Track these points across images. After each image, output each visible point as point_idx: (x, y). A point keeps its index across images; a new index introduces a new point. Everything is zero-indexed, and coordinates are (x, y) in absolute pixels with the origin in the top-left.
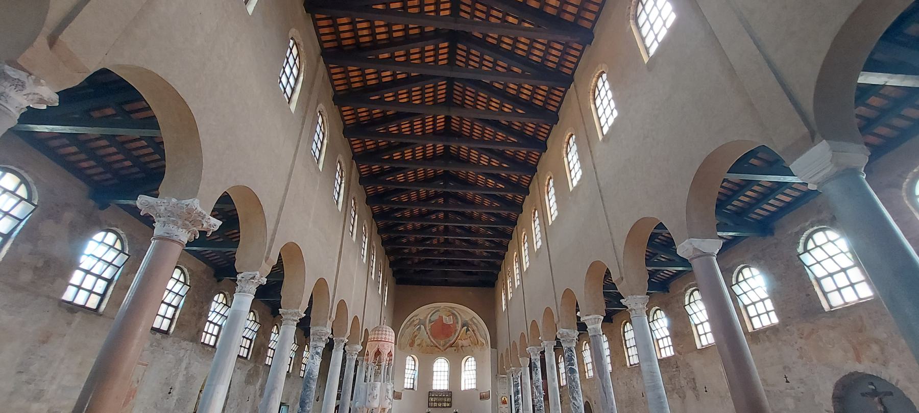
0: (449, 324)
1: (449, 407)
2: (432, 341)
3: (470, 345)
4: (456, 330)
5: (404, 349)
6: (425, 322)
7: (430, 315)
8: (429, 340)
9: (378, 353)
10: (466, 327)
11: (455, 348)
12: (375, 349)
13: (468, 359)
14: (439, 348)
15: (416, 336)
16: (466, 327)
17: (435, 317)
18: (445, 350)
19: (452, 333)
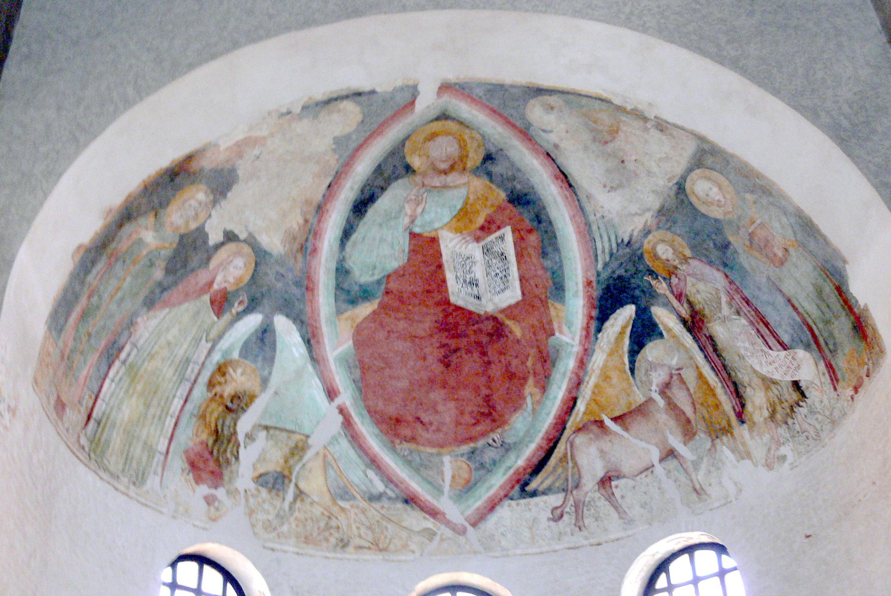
2: (374, 462)
5: (139, 479)
6: (307, 285)
8: (345, 444)
10: (628, 312)
11: (555, 500)
13: (662, 567)
14: (434, 513)
16: (628, 312)
18: (478, 520)
19: (525, 379)
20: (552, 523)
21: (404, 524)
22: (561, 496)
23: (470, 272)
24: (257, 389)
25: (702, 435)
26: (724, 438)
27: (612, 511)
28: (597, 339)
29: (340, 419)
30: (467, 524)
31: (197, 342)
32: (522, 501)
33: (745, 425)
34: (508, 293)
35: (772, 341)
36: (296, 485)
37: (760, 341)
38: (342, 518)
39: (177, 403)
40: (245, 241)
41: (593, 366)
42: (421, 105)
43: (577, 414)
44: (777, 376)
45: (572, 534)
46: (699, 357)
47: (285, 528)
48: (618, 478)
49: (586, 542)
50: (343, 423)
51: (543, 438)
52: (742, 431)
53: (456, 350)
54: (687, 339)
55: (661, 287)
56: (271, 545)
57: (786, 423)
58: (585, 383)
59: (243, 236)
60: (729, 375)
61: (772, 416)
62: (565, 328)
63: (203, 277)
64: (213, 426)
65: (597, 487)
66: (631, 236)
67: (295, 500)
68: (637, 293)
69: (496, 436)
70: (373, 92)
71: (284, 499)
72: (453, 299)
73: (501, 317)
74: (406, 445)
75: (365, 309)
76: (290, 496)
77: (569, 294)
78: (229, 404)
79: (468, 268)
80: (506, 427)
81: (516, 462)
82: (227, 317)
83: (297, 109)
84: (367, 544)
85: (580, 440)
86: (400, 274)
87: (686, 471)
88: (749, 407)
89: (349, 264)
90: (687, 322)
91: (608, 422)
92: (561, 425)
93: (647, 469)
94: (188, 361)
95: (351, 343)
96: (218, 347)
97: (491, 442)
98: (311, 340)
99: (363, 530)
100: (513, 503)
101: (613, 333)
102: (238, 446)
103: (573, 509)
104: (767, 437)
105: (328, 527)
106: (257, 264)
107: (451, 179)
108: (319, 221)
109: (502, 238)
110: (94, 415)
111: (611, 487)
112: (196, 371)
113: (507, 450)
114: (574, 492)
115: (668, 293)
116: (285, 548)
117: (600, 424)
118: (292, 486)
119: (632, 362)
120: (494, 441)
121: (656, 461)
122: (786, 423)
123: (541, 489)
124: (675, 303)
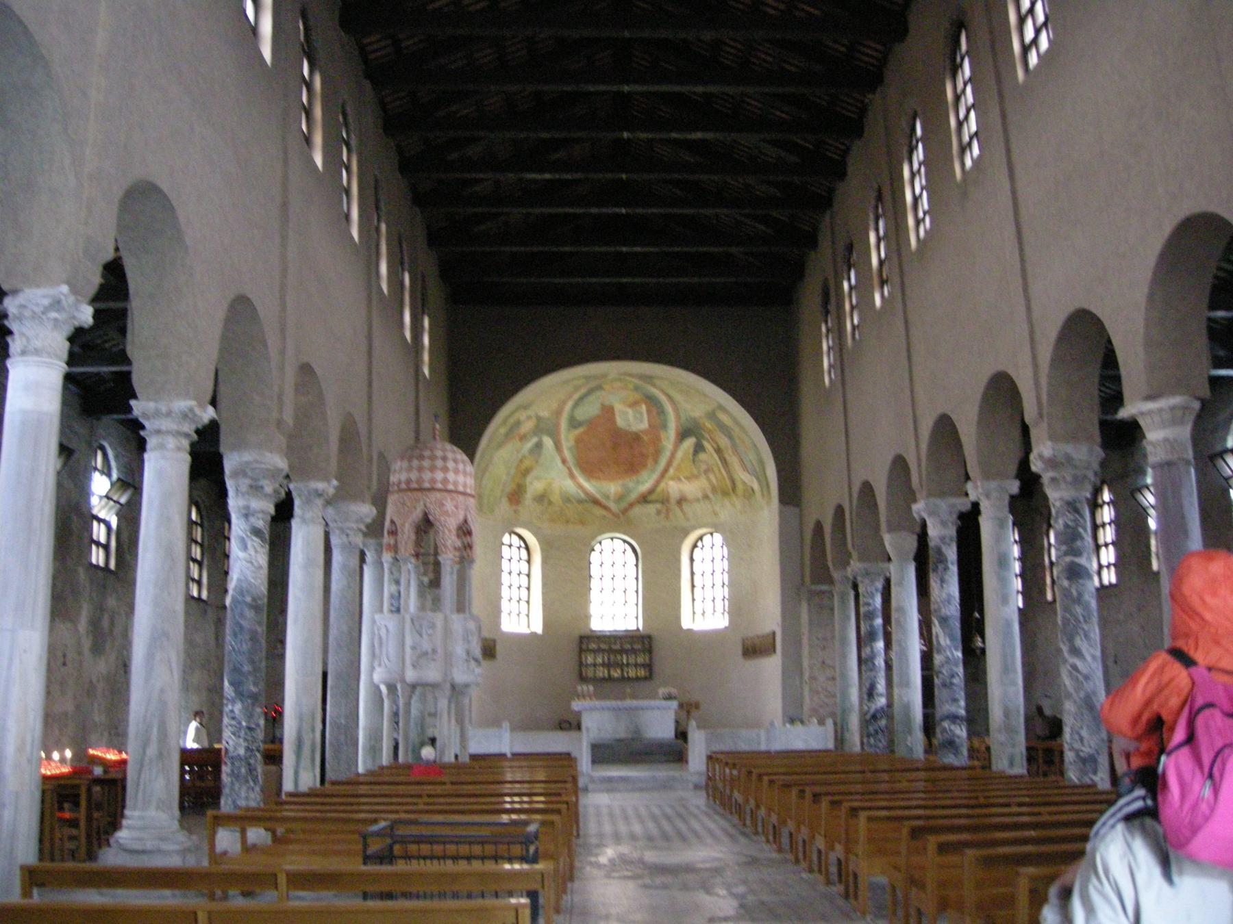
1: (646, 678)
2: (581, 487)
3: (706, 497)
4: (658, 453)
6: (557, 425)
7: (570, 404)
9: (426, 525)
11: (658, 506)
12: (417, 514)
14: (606, 508)
15: (527, 471)
17: (590, 410)
18: (625, 511)
29: (567, 471)
44: (746, 481)
46: (719, 463)
54: (715, 456)
55: (707, 436)
85: (671, 483)
121: (701, 498)
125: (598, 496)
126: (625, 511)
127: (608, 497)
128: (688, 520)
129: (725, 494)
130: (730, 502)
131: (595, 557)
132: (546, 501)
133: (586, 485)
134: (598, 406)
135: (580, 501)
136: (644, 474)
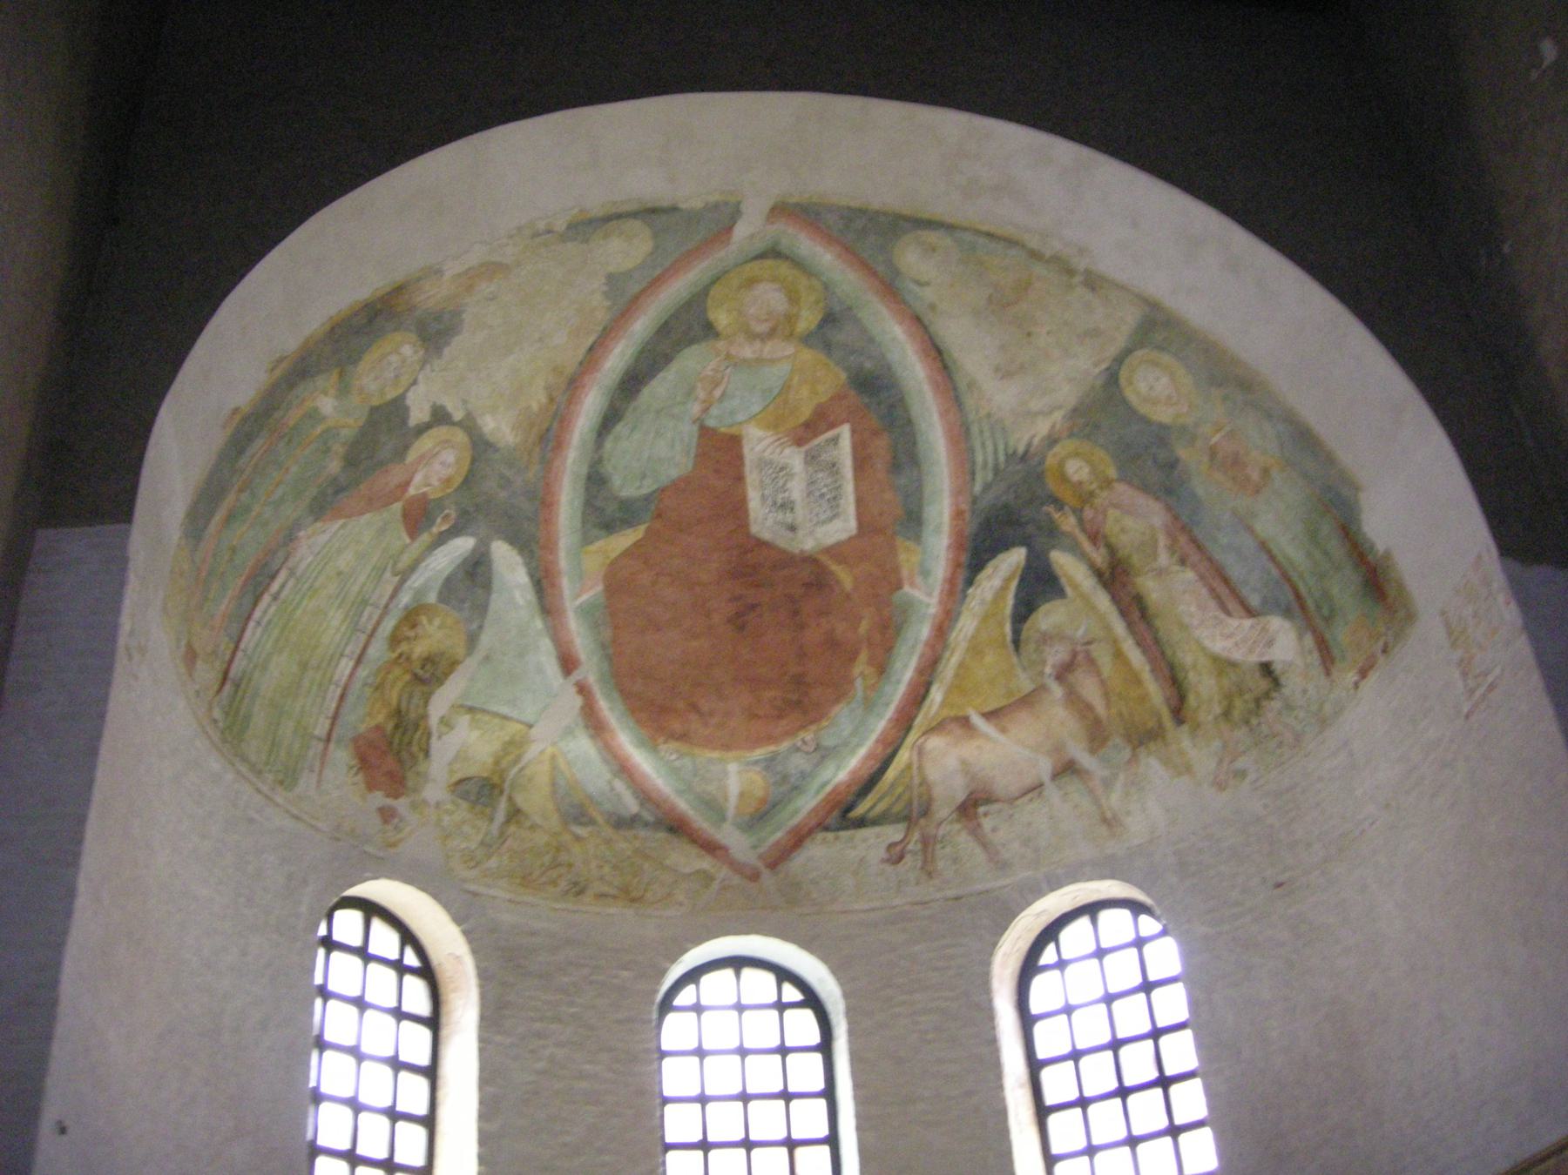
0: (807, 543)
2: (624, 769)
3: (1067, 769)
4: (889, 631)
5: (288, 778)
7: (591, 404)
10: (1015, 558)
11: (894, 833)
13: (1050, 933)
14: (711, 847)
16: (1015, 558)
18: (778, 858)
20: (889, 868)
21: (668, 862)
22: (902, 827)
23: (783, 489)
24: (460, 651)
25: (1118, 740)
26: (1152, 746)
27: (978, 850)
28: (965, 596)
29: (578, 701)
30: (760, 865)
31: (380, 571)
32: (844, 834)
33: (1185, 728)
34: (837, 524)
35: (1232, 605)
36: (510, 799)
37: (1212, 604)
38: (576, 849)
39: (346, 666)
40: (459, 424)
41: (958, 635)
42: (741, 231)
43: (930, 707)
44: (1237, 656)
45: (917, 884)
46: (1119, 627)
47: (493, 863)
48: (989, 799)
49: (939, 895)
50: (582, 708)
51: (878, 741)
52: (1182, 739)
53: (753, 607)
54: (1103, 601)
55: (1068, 523)
56: (473, 887)
57: (1247, 722)
58: (944, 661)
59: (458, 415)
60: (1163, 653)
61: (1227, 714)
62: (919, 580)
63: (396, 475)
64: (394, 702)
65: (954, 815)
66: (1029, 445)
67: (508, 821)
68: (1030, 529)
69: (808, 735)
70: (674, 209)
71: (491, 820)
72: (755, 529)
73: (824, 559)
74: (673, 745)
75: (625, 540)
76: (500, 816)
77: (928, 532)
78: (420, 672)
79: (781, 483)
80: (825, 723)
81: (835, 775)
82: (425, 538)
83: (560, 225)
84: (612, 891)
85: (935, 743)
86: (679, 487)
87: (1091, 791)
88: (1192, 700)
89: (608, 468)
90: (1104, 573)
91: (977, 720)
92: (904, 721)
93: (1034, 789)
94: (365, 602)
95: (600, 588)
96: (409, 583)
97: (799, 744)
98: (543, 583)
99: (607, 869)
100: (830, 836)
101: (992, 587)
102: (429, 735)
103: (919, 846)
104: (1217, 744)
105: (555, 865)
106: (474, 460)
107: (770, 349)
108: (570, 402)
109: (835, 441)
110: (232, 674)
111: (976, 813)
112: (375, 617)
113: (823, 757)
114: (922, 822)
115: (1077, 532)
116: (492, 892)
117: (965, 722)
118: (504, 800)
119: (1017, 633)
120: (804, 742)
121: (1046, 778)
122: (1247, 722)
123: (872, 814)
124: (1086, 545)
125: (683, 805)
126: (778, 858)
127: (713, 807)
128: (1003, 866)
129: (1144, 737)
130: (1167, 762)
131: (676, 1031)
132: (503, 806)
133: (642, 760)
134: (689, 431)
135: (623, 823)
136: (843, 717)
